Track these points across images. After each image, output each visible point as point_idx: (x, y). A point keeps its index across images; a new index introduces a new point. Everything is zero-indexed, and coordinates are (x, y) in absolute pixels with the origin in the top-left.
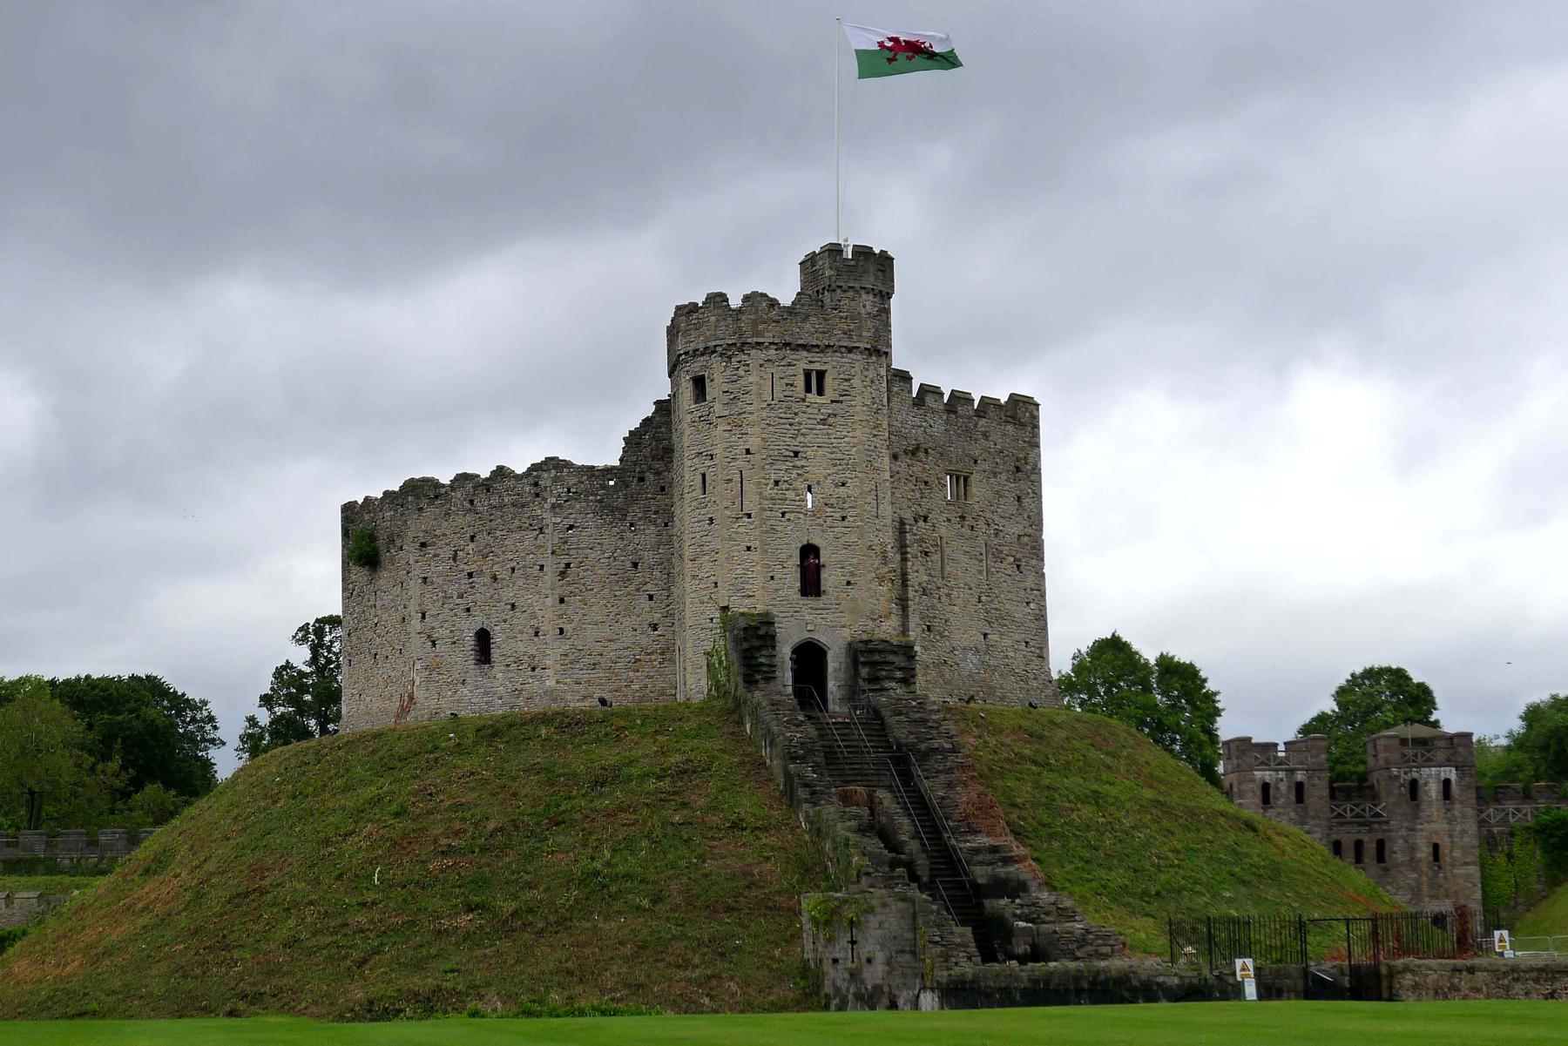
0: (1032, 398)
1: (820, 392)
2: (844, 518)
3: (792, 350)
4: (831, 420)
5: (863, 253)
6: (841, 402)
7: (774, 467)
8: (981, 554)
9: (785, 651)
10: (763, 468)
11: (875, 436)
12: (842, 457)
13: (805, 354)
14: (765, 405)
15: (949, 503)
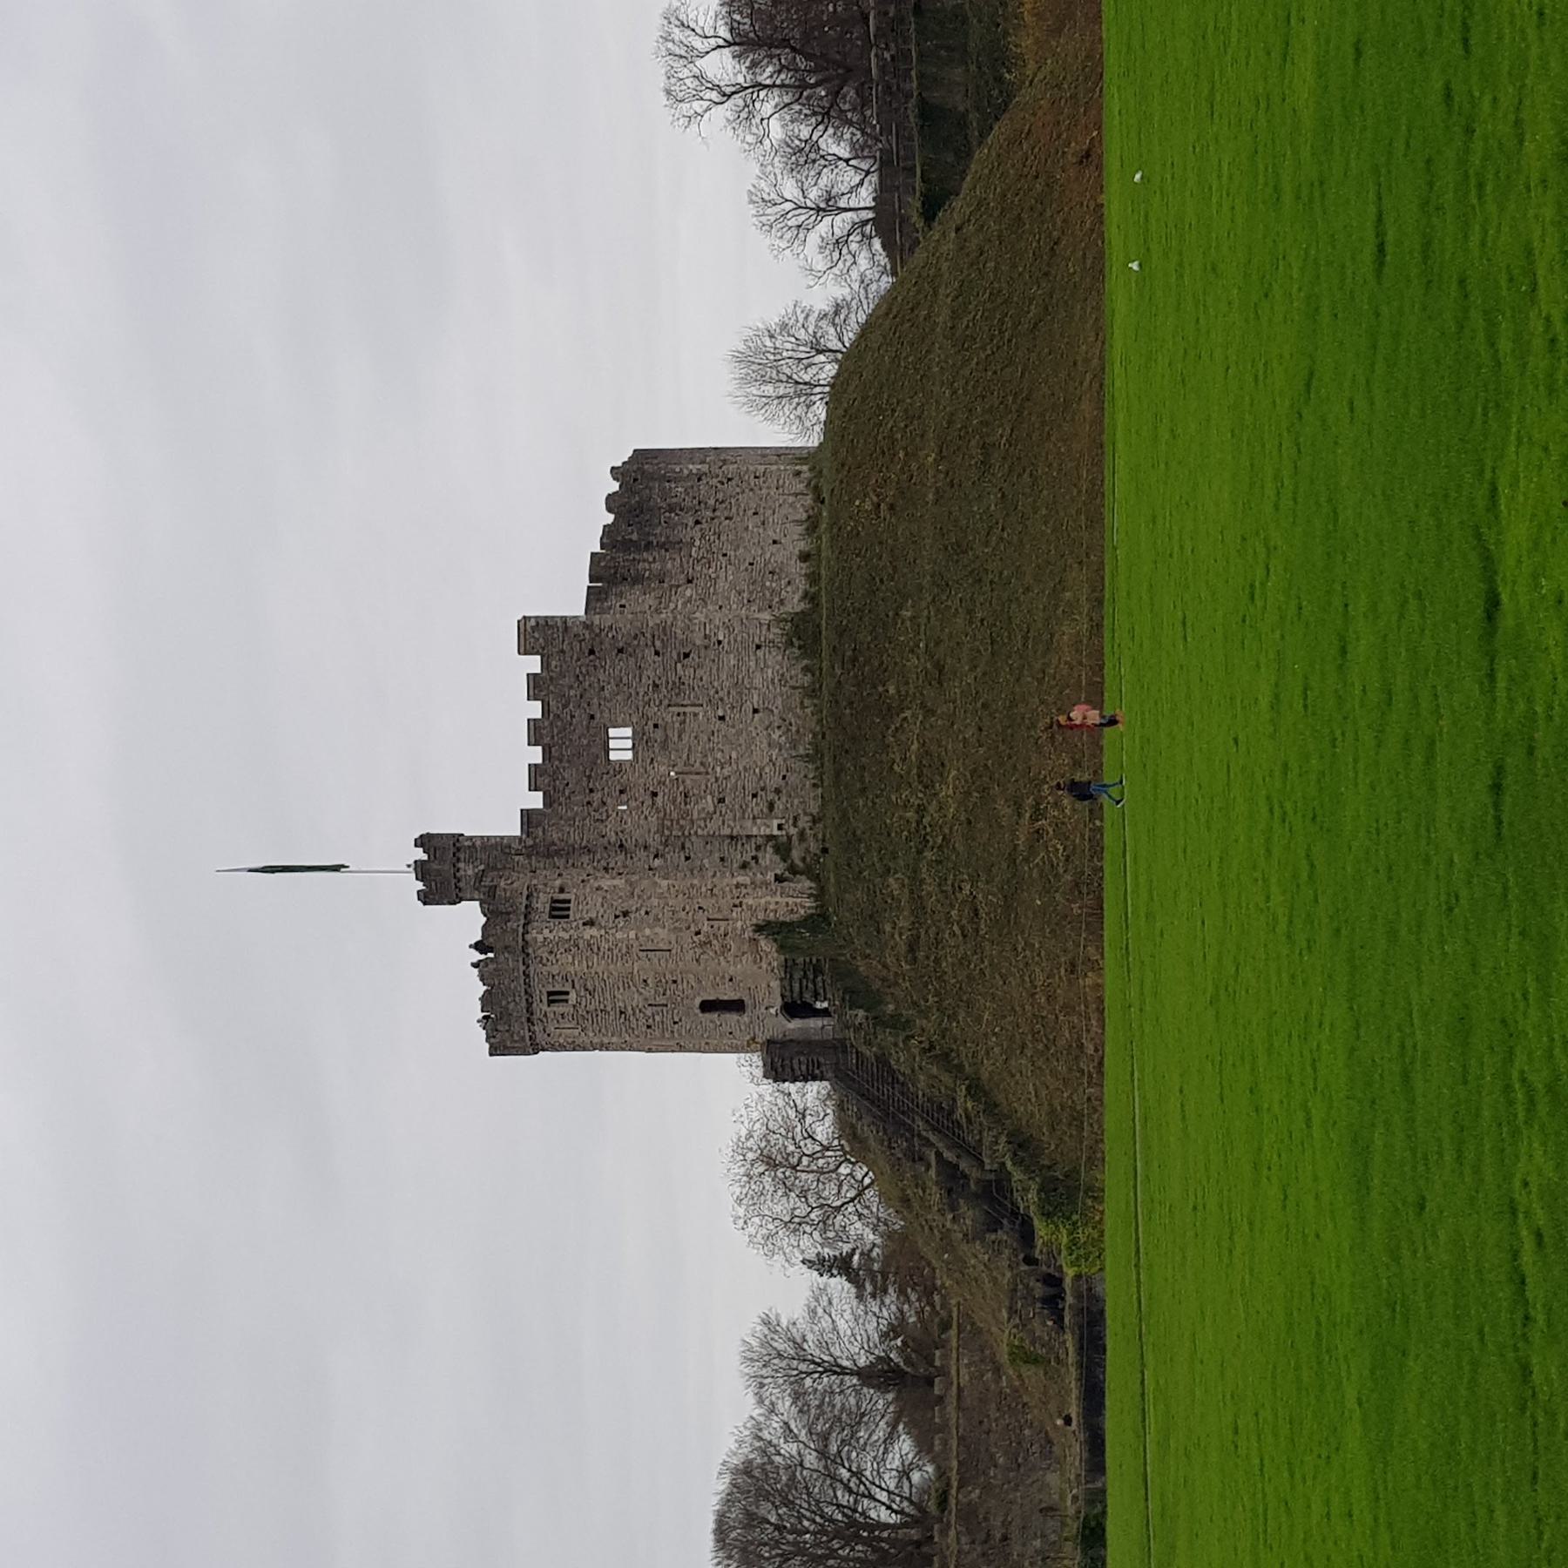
0: (519, 622)
1: (567, 993)
2: (675, 982)
3: (532, 1014)
4: (591, 988)
5: (421, 870)
6: (573, 981)
7: (635, 1027)
8: (679, 714)
9: (796, 1024)
10: (638, 1037)
11: (599, 949)
12: (621, 986)
13: (534, 1005)
14: (583, 1034)
15: (635, 755)
